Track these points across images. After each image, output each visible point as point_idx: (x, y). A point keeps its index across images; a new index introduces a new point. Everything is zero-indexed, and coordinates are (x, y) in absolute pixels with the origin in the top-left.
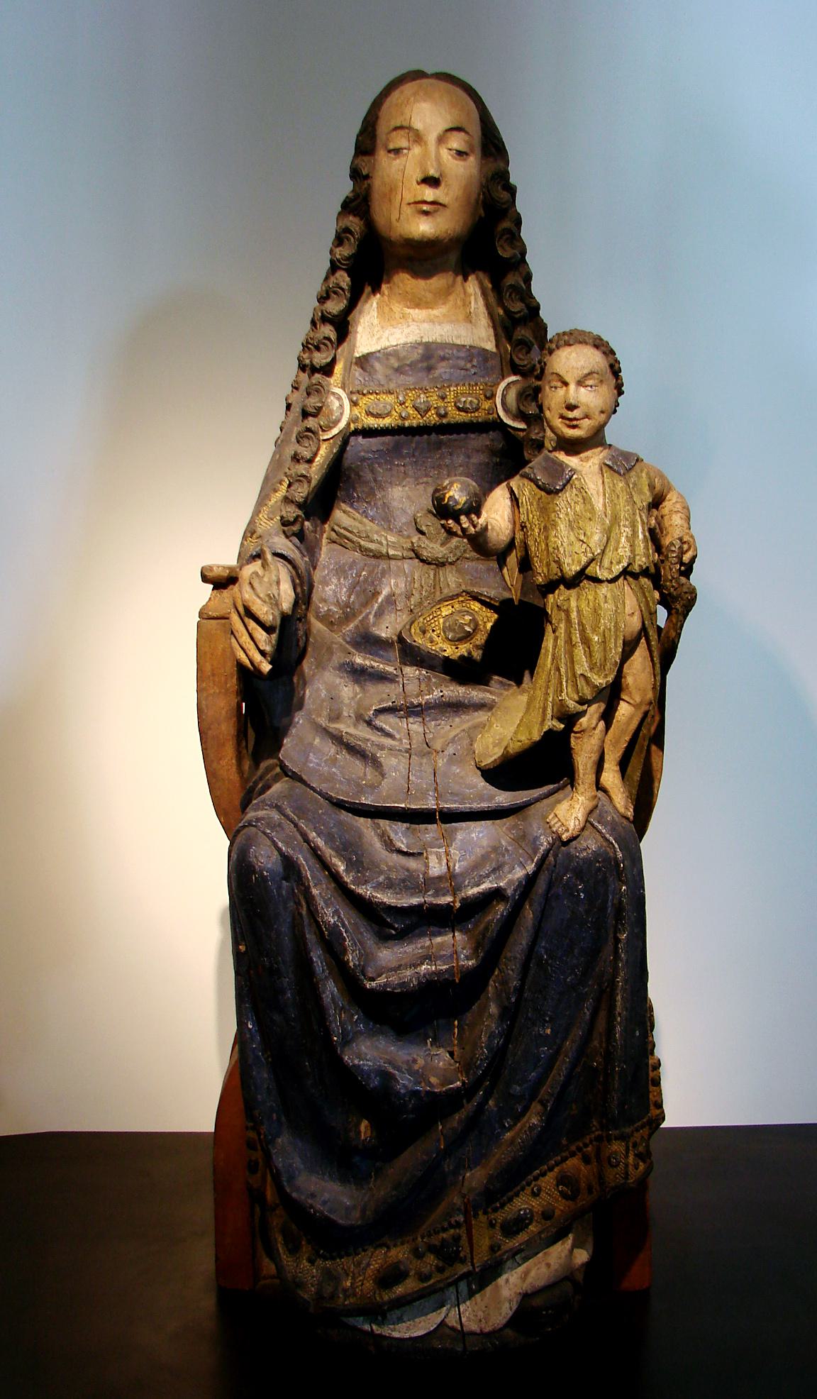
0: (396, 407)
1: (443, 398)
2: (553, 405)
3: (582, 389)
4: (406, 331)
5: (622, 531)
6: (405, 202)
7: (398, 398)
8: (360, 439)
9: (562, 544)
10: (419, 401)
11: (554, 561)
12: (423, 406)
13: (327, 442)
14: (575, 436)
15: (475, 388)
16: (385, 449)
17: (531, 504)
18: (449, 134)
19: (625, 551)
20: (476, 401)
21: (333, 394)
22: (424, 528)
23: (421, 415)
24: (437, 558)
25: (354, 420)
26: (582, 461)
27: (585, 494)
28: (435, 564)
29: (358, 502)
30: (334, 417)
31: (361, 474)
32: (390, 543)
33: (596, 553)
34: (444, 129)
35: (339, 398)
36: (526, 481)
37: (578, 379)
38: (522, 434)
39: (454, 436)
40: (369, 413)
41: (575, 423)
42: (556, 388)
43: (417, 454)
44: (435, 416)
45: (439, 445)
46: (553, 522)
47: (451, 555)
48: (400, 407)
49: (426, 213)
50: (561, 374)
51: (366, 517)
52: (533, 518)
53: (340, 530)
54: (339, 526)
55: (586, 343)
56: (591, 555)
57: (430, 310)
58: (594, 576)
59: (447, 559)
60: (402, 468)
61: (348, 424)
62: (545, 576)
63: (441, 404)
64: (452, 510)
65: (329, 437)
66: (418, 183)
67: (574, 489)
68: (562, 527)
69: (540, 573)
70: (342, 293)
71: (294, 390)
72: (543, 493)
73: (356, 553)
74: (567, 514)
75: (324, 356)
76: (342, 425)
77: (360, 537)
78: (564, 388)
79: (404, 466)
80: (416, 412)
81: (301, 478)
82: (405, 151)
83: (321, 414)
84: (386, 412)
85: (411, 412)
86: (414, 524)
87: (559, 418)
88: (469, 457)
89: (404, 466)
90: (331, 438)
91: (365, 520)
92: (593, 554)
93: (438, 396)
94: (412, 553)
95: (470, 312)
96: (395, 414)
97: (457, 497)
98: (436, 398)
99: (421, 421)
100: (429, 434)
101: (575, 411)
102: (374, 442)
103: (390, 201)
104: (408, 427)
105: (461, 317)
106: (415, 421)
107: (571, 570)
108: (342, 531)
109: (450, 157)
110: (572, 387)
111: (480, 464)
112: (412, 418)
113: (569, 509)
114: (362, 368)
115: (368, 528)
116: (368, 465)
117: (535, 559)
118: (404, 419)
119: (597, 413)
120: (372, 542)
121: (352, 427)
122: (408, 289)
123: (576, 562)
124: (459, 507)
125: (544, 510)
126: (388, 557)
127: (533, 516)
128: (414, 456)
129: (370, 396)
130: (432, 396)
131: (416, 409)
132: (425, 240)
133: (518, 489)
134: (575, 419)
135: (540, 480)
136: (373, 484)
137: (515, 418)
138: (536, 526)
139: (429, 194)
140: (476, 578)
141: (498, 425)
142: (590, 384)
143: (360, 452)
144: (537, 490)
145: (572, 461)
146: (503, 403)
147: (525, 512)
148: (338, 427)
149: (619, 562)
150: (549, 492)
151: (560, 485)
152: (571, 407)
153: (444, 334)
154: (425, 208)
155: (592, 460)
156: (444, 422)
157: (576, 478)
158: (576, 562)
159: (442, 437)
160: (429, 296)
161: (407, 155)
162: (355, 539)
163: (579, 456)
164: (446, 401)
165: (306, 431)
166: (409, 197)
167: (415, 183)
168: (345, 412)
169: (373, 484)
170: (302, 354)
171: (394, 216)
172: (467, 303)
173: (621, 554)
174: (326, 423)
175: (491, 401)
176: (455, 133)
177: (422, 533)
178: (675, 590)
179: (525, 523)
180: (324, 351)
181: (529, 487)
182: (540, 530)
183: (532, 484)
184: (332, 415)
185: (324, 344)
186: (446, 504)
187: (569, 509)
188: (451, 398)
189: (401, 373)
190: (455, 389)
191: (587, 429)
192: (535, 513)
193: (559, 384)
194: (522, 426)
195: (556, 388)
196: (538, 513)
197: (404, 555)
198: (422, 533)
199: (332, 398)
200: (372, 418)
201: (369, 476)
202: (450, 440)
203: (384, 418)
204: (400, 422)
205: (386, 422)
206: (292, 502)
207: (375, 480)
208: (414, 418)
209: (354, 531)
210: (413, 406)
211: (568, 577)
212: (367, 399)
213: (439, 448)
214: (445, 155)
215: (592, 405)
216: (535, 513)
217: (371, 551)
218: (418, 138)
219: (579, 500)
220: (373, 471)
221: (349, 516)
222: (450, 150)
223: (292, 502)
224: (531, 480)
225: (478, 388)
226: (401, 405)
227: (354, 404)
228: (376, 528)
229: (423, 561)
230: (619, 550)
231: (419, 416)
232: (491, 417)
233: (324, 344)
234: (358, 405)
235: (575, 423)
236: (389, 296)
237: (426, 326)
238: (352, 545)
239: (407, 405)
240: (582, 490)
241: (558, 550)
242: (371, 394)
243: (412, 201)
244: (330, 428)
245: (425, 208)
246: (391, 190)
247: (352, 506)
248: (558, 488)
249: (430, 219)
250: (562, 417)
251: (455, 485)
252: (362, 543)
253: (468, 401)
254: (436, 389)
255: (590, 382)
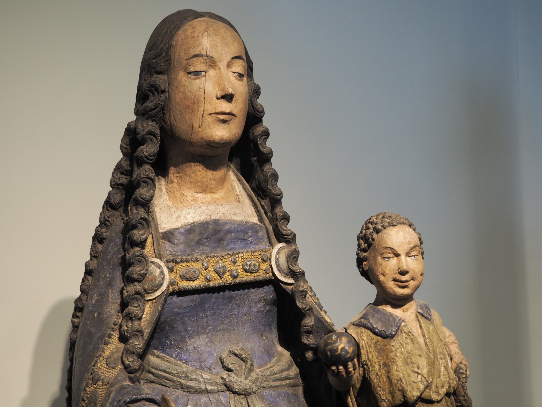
0: (202, 271)
1: (234, 263)
2: (387, 271)
3: (408, 259)
4: (199, 211)
5: (441, 363)
6: (207, 112)
7: (203, 264)
8: (175, 298)
9: (404, 377)
10: (218, 266)
11: (399, 390)
12: (221, 270)
13: (150, 302)
14: (405, 294)
15: (255, 254)
16: (193, 305)
17: (370, 346)
18: (233, 61)
19: (446, 378)
20: (257, 264)
21: (153, 263)
22: (231, 366)
23: (220, 277)
24: (246, 389)
25: (172, 283)
26: (404, 311)
27: (412, 337)
28: (245, 395)
29: (170, 348)
30: (157, 282)
31: (175, 325)
32: (206, 381)
33: (430, 381)
34: (231, 58)
35: (159, 266)
36: (363, 330)
37: (406, 251)
38: (290, 287)
39: (241, 292)
40: (183, 278)
41: (406, 284)
42: (389, 258)
43: (215, 307)
44: (229, 277)
45: (231, 298)
46: (393, 360)
47: (254, 386)
48: (205, 271)
49: (224, 121)
50: (394, 247)
51: (180, 360)
52: (373, 357)
53: (158, 372)
54: (157, 369)
55: (404, 224)
56: (427, 383)
57: (213, 194)
58: (429, 398)
59: (252, 390)
60: (205, 319)
61: (168, 287)
62: (390, 402)
63: (233, 267)
64: (343, 358)
65: (152, 298)
66: (218, 98)
67: (404, 334)
68: (400, 363)
69: (384, 400)
70: (151, 182)
71: (93, 258)
72: (379, 338)
73: (177, 390)
74: (402, 353)
75: (141, 232)
76: (164, 287)
77: (180, 377)
78: (396, 258)
79: (206, 317)
80: (217, 275)
81: (137, 333)
82: (203, 73)
83: (145, 279)
84: (196, 276)
85: (213, 275)
86: (220, 363)
87: (392, 281)
88: (250, 307)
89: (206, 317)
90: (154, 299)
91: (179, 362)
92: (428, 382)
93: (231, 261)
94: (224, 387)
95: (237, 195)
96: (202, 277)
97: (347, 348)
98: (230, 263)
99: (221, 282)
100: (224, 291)
101: (407, 275)
102: (185, 300)
103: (193, 111)
104: (218, 286)
105: (233, 199)
106: (216, 282)
107: (413, 396)
108: (160, 373)
109: (234, 78)
110: (403, 257)
111: (258, 312)
112: (214, 280)
113: (403, 349)
114: (170, 241)
115: (185, 369)
116: (181, 319)
117: (379, 389)
118: (208, 280)
119: (419, 276)
120: (192, 380)
121: (171, 289)
122: (199, 179)
123: (416, 389)
124: (349, 356)
125: (383, 352)
126: (207, 392)
127: (373, 356)
128: (213, 309)
129: (182, 264)
130: (226, 262)
131: (216, 273)
132: (223, 141)
133: (357, 335)
134: (407, 281)
135: (376, 328)
136: (184, 334)
137: (286, 275)
138: (376, 363)
139: (225, 106)
140: (272, 402)
141: (274, 282)
142: (414, 255)
143: (174, 308)
144: (373, 336)
145: (397, 312)
146: (278, 265)
147: (365, 353)
148: (161, 289)
149: (443, 387)
150: (384, 337)
151: (394, 331)
152: (403, 273)
153: (225, 212)
154: (222, 117)
155: (410, 310)
156: (237, 281)
157: (404, 325)
158: (416, 389)
159: (232, 293)
160: (214, 183)
161: (205, 76)
162: (175, 379)
163: (402, 308)
164: (236, 265)
165: (135, 294)
166: (210, 109)
167: (215, 98)
168: (166, 278)
169: (184, 334)
170: (100, 229)
171: (196, 125)
172: (234, 188)
173: (444, 380)
174: (150, 286)
175: (266, 263)
176: (237, 60)
177: (229, 370)
178: (466, 402)
179: (366, 361)
180: (140, 229)
181: (366, 334)
182: (380, 366)
183: (369, 331)
184: (155, 280)
185: (141, 224)
186: (339, 354)
187: (403, 349)
188: (239, 262)
189: (201, 244)
190: (242, 255)
191: (412, 288)
192: (373, 353)
193: (392, 255)
194: (291, 281)
195: (389, 258)
196: (376, 353)
197: (219, 389)
198: (229, 370)
199: (153, 266)
200: (185, 281)
201: (181, 328)
202: (238, 295)
203: (194, 281)
204: (206, 283)
205: (196, 284)
206: (134, 353)
207: (186, 330)
208: (215, 279)
209: (173, 372)
210: (214, 270)
211: (411, 401)
212: (180, 266)
213: (230, 302)
214: (232, 78)
215: (416, 270)
216: (373, 353)
217: (192, 388)
218: (212, 63)
219: (409, 341)
220: (183, 323)
221: (163, 360)
222: (234, 72)
223: (134, 353)
224: (367, 328)
225: (257, 253)
226: (205, 269)
227: (171, 270)
228: (191, 368)
229: (235, 393)
230: (442, 377)
231: (219, 278)
232: (268, 275)
233: (141, 224)
234: (173, 271)
235: (406, 284)
236: (178, 183)
237: (211, 207)
238: (172, 384)
239: (210, 269)
240: (409, 334)
241: (401, 381)
242: (183, 262)
243: (213, 112)
244: (155, 291)
245: (222, 117)
246: (194, 103)
247: (164, 352)
248: (393, 333)
249: (226, 126)
250: (395, 280)
251: (343, 339)
252: (183, 382)
253: (252, 264)
254: (229, 256)
255: (413, 254)
